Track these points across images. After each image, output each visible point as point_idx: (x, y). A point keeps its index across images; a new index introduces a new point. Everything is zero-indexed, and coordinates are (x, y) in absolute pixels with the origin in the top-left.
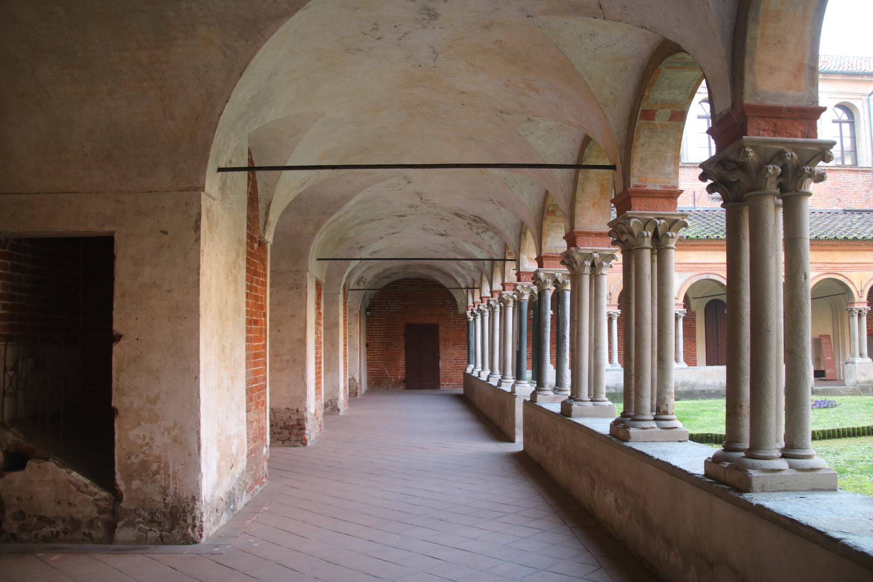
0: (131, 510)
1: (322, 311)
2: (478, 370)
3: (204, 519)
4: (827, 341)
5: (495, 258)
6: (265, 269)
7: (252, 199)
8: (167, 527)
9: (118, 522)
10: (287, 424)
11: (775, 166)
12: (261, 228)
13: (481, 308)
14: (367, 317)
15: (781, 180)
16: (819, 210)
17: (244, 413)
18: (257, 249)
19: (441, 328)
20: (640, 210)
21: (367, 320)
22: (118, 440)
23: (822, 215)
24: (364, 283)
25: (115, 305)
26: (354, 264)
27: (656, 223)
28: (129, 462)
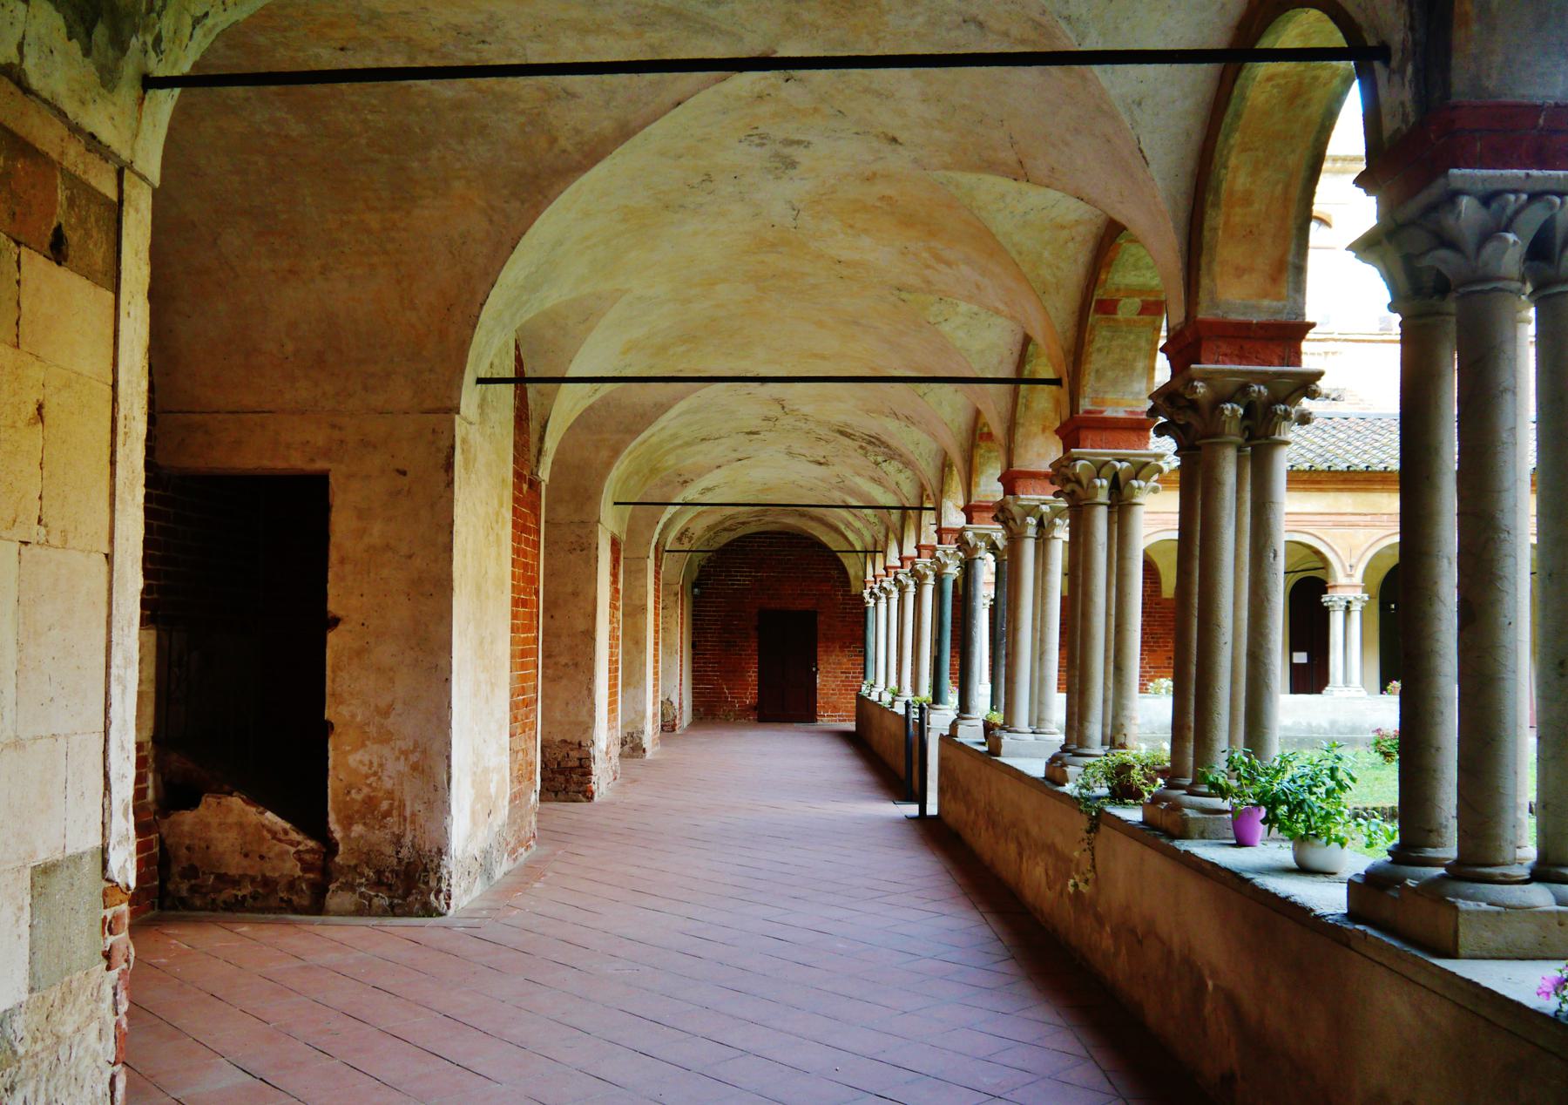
0: (349, 866)
1: (620, 586)
2: (879, 690)
3: (453, 882)
5: (908, 505)
6: (538, 522)
7: (521, 417)
8: (400, 892)
9: (330, 883)
10: (563, 765)
11: (1235, 406)
12: (533, 459)
13: (884, 585)
14: (695, 597)
15: (1247, 423)
18: (527, 492)
19: (820, 618)
20: (1092, 447)
21: (694, 602)
22: (334, 768)
24: (691, 539)
25: (331, 576)
26: (671, 510)
27: (1114, 466)
28: (348, 799)
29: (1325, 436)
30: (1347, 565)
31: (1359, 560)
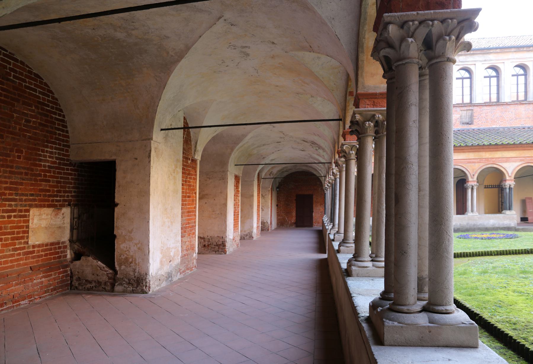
0: (121, 278)
1: (240, 189)
3: (151, 283)
4: (530, 201)
6: (196, 172)
8: (135, 286)
9: (116, 283)
12: (193, 153)
14: (277, 191)
16: (528, 126)
17: (179, 238)
18: (190, 163)
19: (314, 196)
20: (350, 141)
21: (277, 193)
22: (117, 249)
23: (529, 129)
24: (273, 174)
25: (116, 191)
26: (261, 167)
28: (120, 258)
29: (466, 135)
30: (472, 175)
31: (476, 173)
